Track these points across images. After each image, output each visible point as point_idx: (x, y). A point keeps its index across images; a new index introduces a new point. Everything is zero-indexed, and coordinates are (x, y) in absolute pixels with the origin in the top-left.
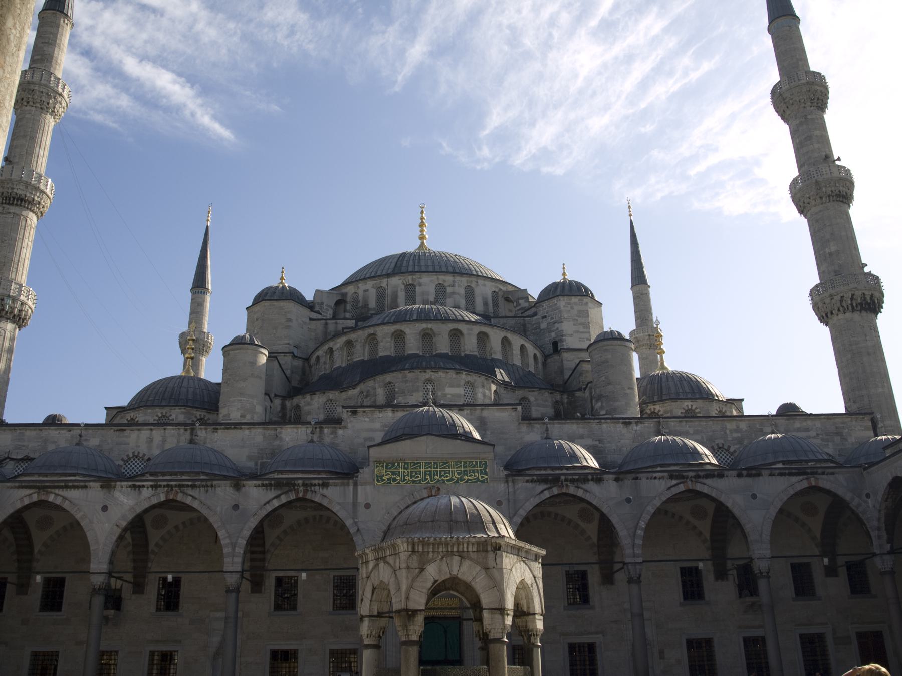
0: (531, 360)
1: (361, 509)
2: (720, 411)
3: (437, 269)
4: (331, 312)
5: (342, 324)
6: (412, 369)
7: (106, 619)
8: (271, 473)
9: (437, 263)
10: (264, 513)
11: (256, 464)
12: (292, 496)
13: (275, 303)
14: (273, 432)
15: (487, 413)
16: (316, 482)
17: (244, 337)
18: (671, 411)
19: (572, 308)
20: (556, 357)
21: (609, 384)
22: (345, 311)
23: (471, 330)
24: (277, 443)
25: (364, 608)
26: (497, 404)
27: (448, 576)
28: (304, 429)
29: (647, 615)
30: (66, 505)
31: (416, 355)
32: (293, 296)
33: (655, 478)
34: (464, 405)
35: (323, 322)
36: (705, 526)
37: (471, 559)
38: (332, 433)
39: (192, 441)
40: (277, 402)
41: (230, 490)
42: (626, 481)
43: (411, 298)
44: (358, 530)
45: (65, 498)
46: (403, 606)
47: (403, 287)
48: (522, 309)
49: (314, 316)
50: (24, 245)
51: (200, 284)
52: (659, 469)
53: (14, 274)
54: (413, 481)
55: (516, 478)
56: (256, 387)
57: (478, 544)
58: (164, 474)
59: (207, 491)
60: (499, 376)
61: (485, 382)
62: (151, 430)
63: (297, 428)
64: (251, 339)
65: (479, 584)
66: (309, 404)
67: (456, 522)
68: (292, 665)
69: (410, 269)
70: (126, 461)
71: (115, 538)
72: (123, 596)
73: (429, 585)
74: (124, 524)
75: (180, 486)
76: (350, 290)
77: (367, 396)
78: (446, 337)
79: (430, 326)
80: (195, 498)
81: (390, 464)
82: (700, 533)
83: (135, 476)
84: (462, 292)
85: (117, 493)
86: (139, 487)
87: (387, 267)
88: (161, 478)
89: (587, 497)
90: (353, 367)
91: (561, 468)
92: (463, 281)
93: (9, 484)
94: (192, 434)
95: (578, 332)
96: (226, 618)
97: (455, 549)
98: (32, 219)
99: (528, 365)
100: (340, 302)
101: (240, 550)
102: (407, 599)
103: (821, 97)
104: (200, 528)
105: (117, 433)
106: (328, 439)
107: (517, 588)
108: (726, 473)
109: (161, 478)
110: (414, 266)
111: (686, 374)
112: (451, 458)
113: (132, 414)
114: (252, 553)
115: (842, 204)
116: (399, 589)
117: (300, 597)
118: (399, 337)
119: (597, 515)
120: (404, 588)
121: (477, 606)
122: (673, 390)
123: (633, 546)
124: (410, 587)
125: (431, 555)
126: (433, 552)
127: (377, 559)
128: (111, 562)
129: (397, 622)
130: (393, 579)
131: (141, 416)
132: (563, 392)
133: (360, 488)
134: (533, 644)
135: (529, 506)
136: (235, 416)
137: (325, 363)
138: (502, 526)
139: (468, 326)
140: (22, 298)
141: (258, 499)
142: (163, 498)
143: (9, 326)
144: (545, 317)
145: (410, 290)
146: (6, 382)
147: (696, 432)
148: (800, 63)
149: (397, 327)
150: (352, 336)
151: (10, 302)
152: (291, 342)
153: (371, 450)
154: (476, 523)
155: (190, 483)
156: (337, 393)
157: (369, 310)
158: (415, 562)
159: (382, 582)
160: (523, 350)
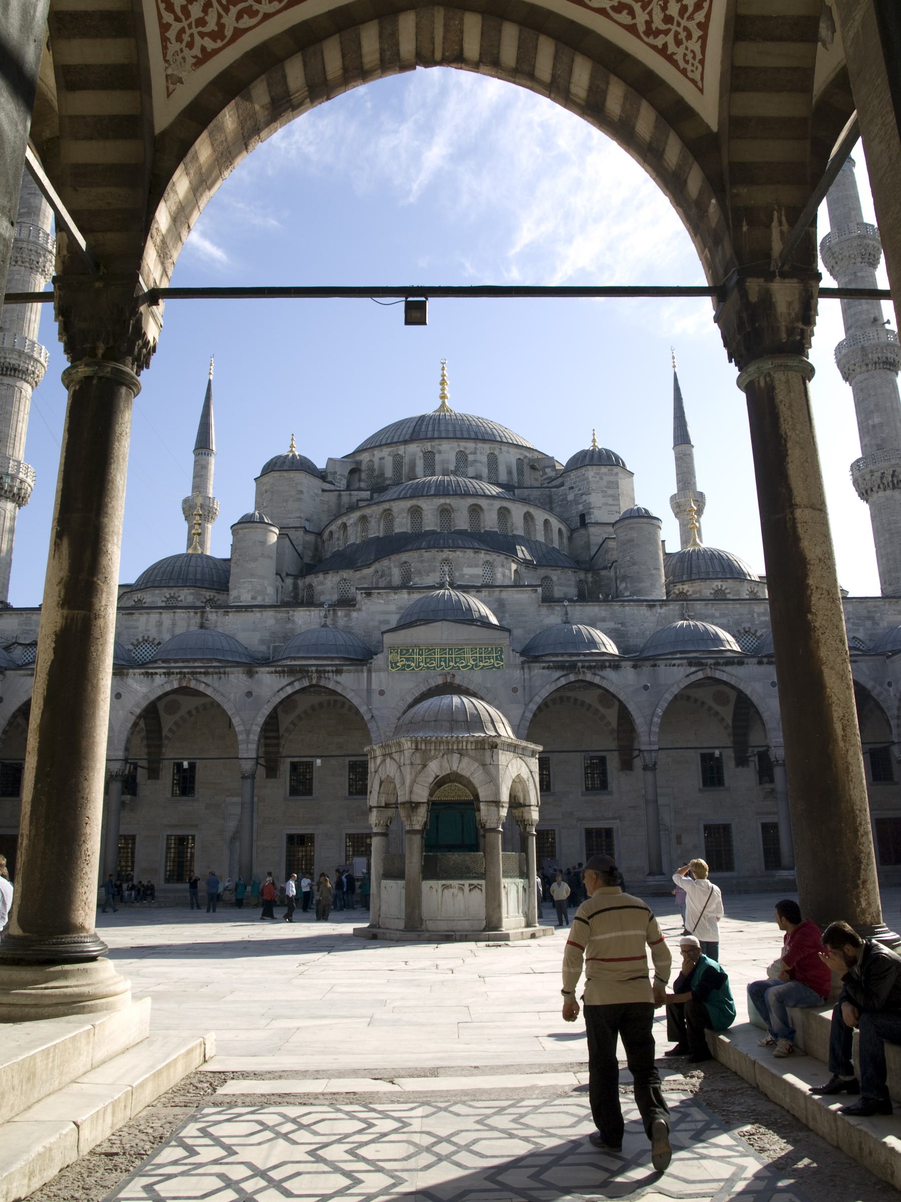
0: (556, 536)
1: (376, 696)
2: (752, 592)
3: (459, 435)
4: (344, 482)
5: (357, 495)
6: (428, 548)
7: (123, 804)
8: (284, 659)
9: (458, 428)
10: (277, 700)
11: (268, 648)
12: (306, 683)
13: (285, 474)
14: (285, 615)
15: (505, 595)
16: (330, 668)
17: (253, 514)
18: (700, 591)
19: (601, 479)
20: (582, 531)
21: (634, 564)
22: (360, 480)
23: (492, 505)
24: (290, 626)
25: (373, 799)
26: (516, 585)
27: (449, 772)
28: (317, 612)
29: (661, 801)
31: (433, 533)
32: (303, 465)
33: (674, 665)
34: (483, 586)
36: (727, 712)
37: (470, 757)
38: (346, 616)
39: (202, 626)
40: (289, 581)
41: (243, 677)
42: (644, 668)
43: (430, 468)
44: (372, 717)
46: (407, 798)
47: (421, 454)
48: (548, 478)
49: (327, 486)
50: (20, 418)
51: (203, 444)
52: (678, 656)
53: (11, 450)
54: (428, 668)
55: (533, 664)
56: (267, 567)
57: (477, 742)
58: (176, 661)
59: (220, 678)
60: (520, 555)
61: (505, 561)
62: (161, 613)
63: (310, 611)
64: (261, 517)
65: (478, 778)
66: (322, 583)
67: (457, 722)
68: (308, 849)
69: (429, 435)
70: (135, 646)
71: (129, 725)
72: (138, 780)
73: (431, 779)
75: (193, 673)
76: (365, 457)
77: (382, 576)
79: (448, 501)
80: (209, 686)
81: (405, 651)
82: (723, 719)
83: (148, 663)
84: (485, 459)
86: (152, 674)
87: (404, 432)
88: (173, 665)
89: (604, 684)
90: (367, 543)
91: (578, 655)
92: (486, 448)
93: (21, 672)
94: (202, 617)
95: (606, 504)
96: (243, 804)
97: (455, 747)
98: (27, 390)
99: (552, 541)
100: (352, 472)
101: (254, 737)
102: (411, 792)
103: (873, 253)
104: (213, 714)
105: (126, 616)
106: (342, 621)
107: (514, 781)
108: (746, 660)
109: (173, 665)
110: (434, 430)
111: (718, 551)
112: (466, 644)
113: (139, 595)
114: (266, 738)
115: (888, 372)
116: (403, 784)
117: (315, 782)
118: (416, 512)
119: (617, 703)
121: (476, 796)
122: (703, 569)
123: (650, 732)
124: (414, 782)
125: (433, 752)
126: (435, 749)
127: (384, 755)
128: (127, 749)
129: (402, 813)
130: (398, 774)
131: (149, 598)
132: (587, 570)
133: (373, 674)
134: (528, 833)
135: (544, 693)
136: (246, 598)
137: (338, 539)
138: (501, 725)
139: (488, 501)
140: (21, 475)
141: (271, 686)
142: (176, 686)
143: (10, 506)
144: (572, 488)
145: (429, 457)
146: (9, 564)
147: (723, 615)
148: (853, 213)
149: (414, 502)
150: (367, 512)
151: (8, 480)
153: (386, 636)
154: (476, 722)
155: (203, 670)
156: (351, 572)
157: (385, 479)
158: (418, 759)
159: (388, 776)
160: (547, 526)
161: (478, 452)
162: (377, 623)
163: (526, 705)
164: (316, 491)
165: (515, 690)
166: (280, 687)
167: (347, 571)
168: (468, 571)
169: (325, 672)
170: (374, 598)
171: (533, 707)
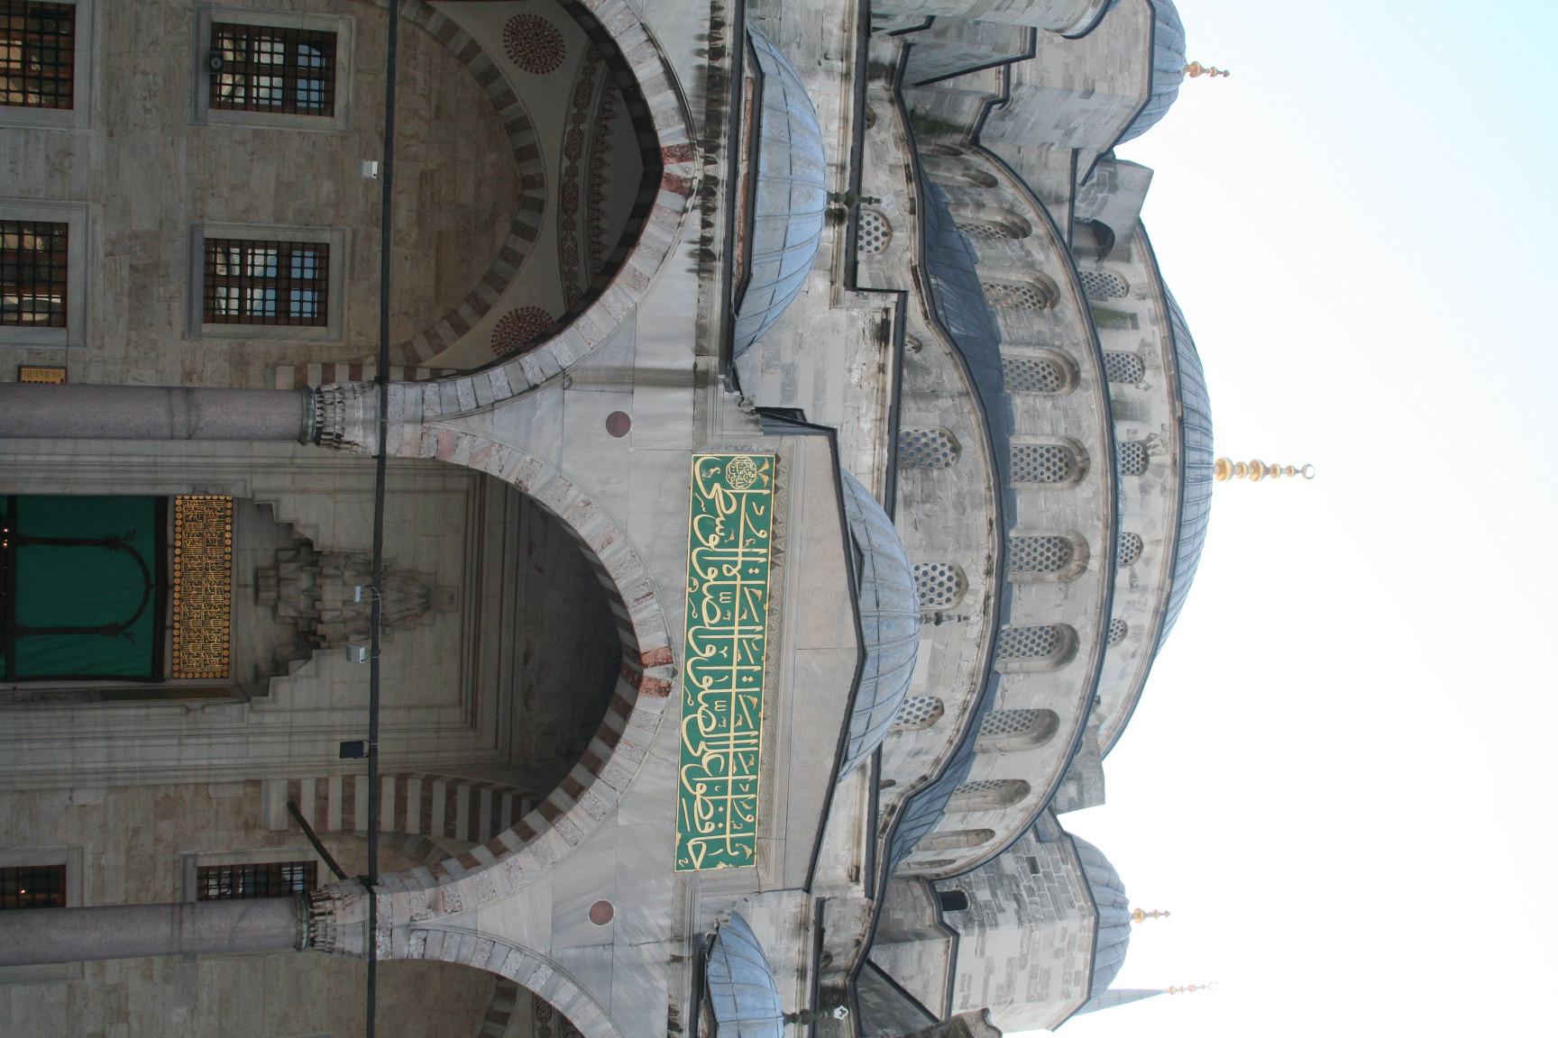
1: (606, 403)
12: (670, 133)
14: (834, 45)
19: (1058, 953)
20: (929, 914)
24: (798, 58)
35: (1067, 194)
47: (1142, 436)
49: (1084, 164)
54: (697, 598)
55: (688, 974)
61: (930, 758)
76: (1135, 273)
78: (1054, 618)
79: (1095, 564)
81: (765, 514)
95: (989, 970)
100: (1103, 239)
112: (772, 738)
118: (1070, 463)
132: (854, 975)
133: (686, 395)
137: (980, 206)
149: (1098, 460)
150: (1069, 306)
152: (1023, 90)
161: (1136, 596)
162: (786, 358)
164: (1079, 133)
165: (602, 913)
166: (660, 36)
167: (915, 243)
169: (707, 210)
170: (870, 355)
171: (537, 983)
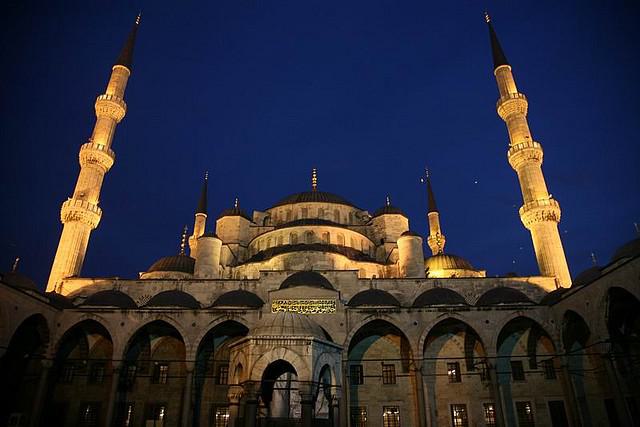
30: (102, 322)
40: (228, 269)
45: (102, 318)
74: (132, 333)
85: (130, 316)
100: (266, 218)
102: (251, 374)
116: (246, 369)
120: (250, 367)
124: (253, 366)
135: (359, 326)
136: (202, 276)
163: (348, 333)
168: (319, 263)
